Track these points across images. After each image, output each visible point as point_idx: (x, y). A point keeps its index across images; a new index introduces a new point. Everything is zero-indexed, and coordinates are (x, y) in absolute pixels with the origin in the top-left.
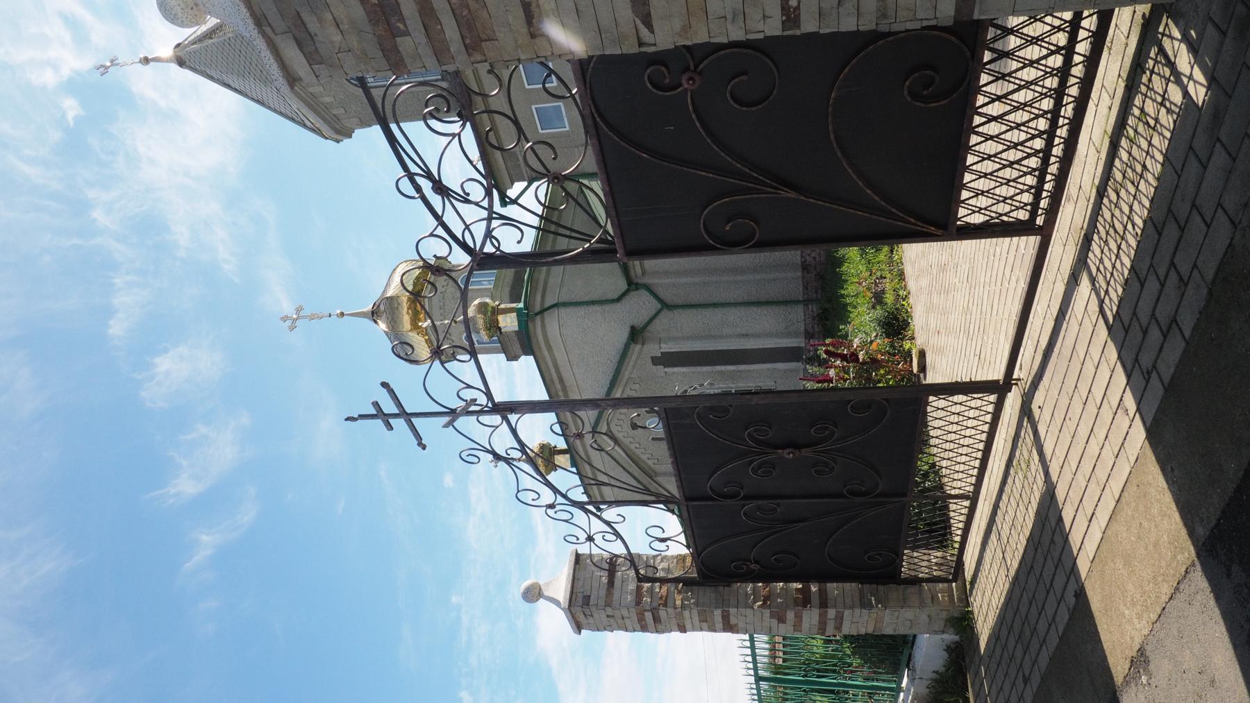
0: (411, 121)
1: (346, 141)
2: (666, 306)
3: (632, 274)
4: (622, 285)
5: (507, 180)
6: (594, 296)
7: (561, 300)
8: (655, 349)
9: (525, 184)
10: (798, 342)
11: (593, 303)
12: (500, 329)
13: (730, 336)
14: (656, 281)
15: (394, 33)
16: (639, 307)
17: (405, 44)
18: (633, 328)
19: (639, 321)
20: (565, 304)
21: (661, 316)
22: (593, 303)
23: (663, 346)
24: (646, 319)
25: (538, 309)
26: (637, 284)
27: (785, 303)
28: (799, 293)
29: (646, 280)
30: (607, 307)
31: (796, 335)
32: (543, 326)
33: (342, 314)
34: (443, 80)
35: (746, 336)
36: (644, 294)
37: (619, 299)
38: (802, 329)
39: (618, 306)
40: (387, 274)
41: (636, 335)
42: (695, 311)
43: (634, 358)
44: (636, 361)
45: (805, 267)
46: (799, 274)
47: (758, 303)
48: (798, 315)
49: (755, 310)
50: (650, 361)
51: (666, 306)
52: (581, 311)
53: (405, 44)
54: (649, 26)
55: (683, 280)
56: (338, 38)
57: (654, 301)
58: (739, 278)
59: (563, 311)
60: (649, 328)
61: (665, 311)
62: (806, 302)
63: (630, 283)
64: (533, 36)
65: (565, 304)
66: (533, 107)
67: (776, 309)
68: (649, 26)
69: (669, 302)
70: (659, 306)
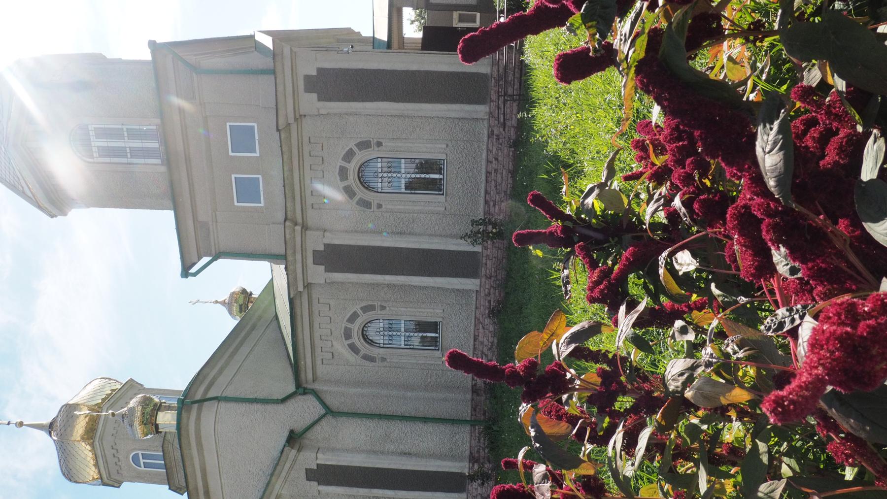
1: (60, 219)
2: (330, 411)
3: (303, 376)
4: (292, 388)
6: (260, 395)
7: (224, 395)
8: (310, 459)
9: (208, 259)
10: (462, 467)
11: (256, 401)
12: (157, 426)
13: (392, 453)
14: (325, 388)
16: (304, 410)
18: (292, 432)
19: (299, 426)
20: (227, 399)
21: (324, 422)
22: (256, 401)
23: (320, 455)
24: (308, 422)
25: (198, 397)
26: (305, 389)
27: (453, 421)
28: (466, 412)
29: (316, 386)
30: (269, 407)
31: (460, 459)
32: (198, 418)
33: (21, 424)
34: (162, 165)
35: (408, 454)
36: (310, 400)
37: (284, 400)
38: (467, 453)
39: (281, 407)
40: (74, 378)
41: (294, 439)
42: (359, 421)
43: (288, 465)
44: (289, 472)
45: (475, 390)
46: (469, 396)
47: (425, 420)
48: (464, 439)
49: (420, 426)
50: (303, 474)
51: (330, 411)
52: (243, 407)
55: (353, 390)
57: (317, 404)
58: (409, 394)
59: (223, 405)
60: (309, 435)
61: (329, 418)
62: (473, 423)
63: (298, 385)
65: (227, 399)
66: (233, 176)
67: (442, 427)
69: (334, 402)
70: (323, 412)
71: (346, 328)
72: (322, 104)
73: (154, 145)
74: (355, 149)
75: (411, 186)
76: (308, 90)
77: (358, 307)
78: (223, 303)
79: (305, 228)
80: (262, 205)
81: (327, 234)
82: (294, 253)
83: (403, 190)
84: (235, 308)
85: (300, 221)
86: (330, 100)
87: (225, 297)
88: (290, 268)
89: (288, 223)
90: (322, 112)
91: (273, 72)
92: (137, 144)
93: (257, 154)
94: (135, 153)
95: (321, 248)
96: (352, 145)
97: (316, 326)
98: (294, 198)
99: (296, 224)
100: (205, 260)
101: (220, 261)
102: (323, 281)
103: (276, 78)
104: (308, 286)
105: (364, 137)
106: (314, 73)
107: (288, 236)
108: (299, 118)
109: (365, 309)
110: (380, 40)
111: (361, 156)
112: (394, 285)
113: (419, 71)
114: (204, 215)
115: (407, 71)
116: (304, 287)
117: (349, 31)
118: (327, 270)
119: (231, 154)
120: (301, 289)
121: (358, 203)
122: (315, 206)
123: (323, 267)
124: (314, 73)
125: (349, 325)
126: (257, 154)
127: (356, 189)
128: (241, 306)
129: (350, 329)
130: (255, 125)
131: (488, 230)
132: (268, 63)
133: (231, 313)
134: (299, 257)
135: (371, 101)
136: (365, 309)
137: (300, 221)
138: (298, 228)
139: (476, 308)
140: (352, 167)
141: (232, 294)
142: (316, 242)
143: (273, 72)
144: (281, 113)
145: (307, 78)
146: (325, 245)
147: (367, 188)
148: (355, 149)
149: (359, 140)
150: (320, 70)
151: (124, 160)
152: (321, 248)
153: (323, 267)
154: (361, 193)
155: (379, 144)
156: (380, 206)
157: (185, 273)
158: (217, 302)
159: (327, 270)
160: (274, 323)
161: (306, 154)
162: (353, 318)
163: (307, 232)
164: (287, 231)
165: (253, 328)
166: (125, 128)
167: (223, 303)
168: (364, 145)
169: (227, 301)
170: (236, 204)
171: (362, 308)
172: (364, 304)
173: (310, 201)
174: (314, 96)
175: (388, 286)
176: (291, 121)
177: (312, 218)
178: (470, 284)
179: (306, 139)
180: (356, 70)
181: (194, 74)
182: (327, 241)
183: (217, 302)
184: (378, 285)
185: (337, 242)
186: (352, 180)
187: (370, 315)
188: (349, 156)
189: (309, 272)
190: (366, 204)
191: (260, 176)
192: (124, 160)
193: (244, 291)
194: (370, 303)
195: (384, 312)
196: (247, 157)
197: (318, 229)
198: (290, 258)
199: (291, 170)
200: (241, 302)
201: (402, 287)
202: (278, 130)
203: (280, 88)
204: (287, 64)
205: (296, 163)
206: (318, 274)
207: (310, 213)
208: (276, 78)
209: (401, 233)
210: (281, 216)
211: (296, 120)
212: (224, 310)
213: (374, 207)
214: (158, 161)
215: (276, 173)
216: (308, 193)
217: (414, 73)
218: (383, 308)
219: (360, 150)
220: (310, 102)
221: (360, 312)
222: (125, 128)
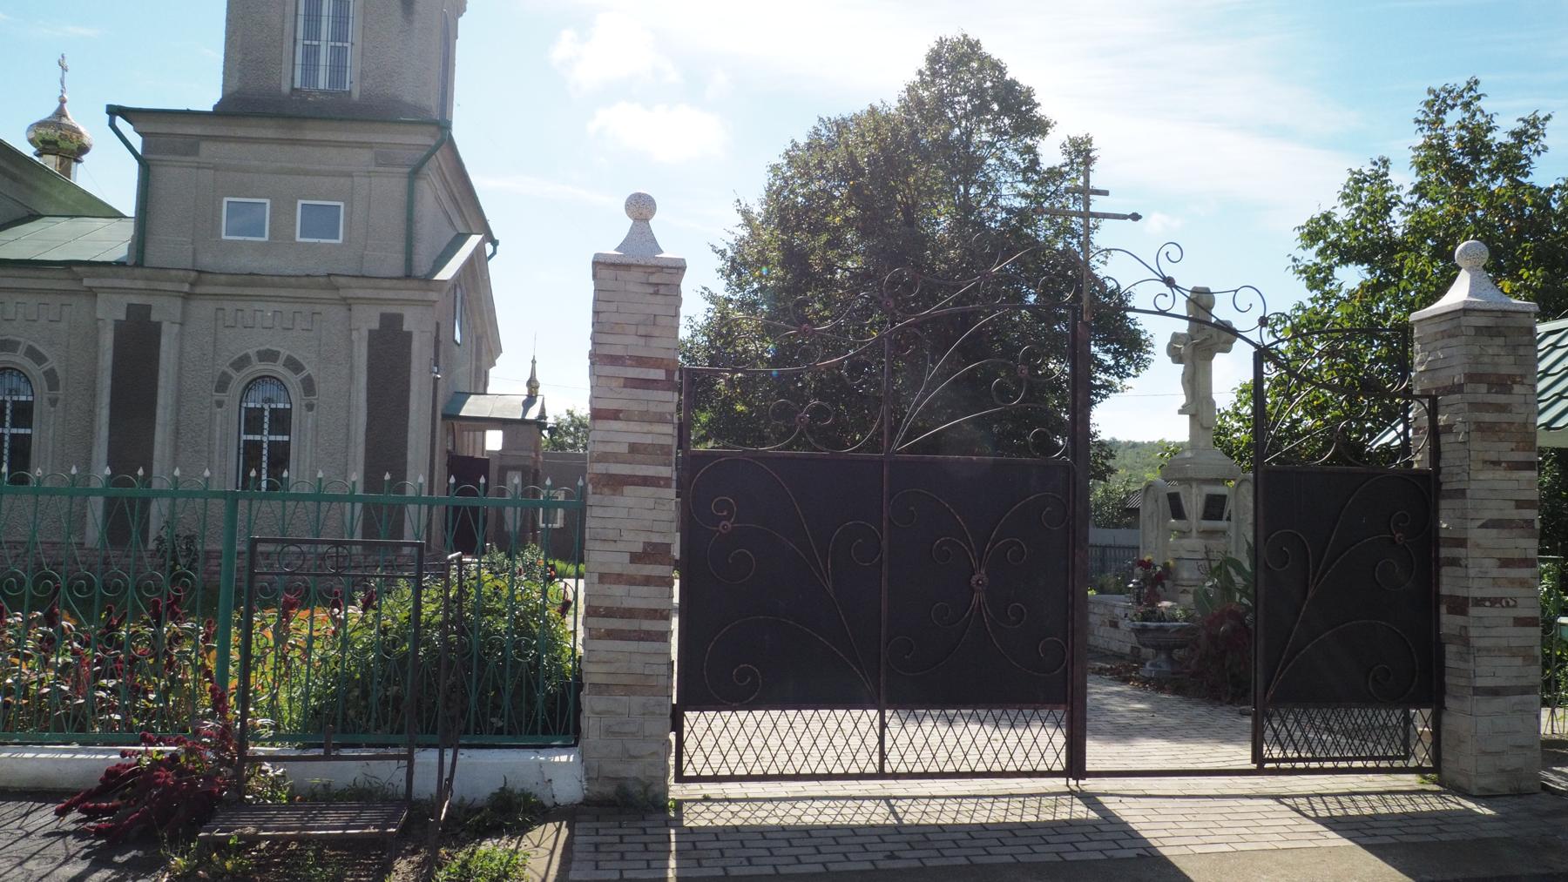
0: (229, 20)
5: (150, 128)
15: (1491, 385)
17: (1483, 388)
34: (293, 89)
53: (1483, 388)
54: (1483, 526)
56: (1490, 351)
64: (1485, 462)
68: (1483, 526)
71: (19, 343)
72: (365, 334)
73: (323, 82)
74: (304, 374)
75: (251, 453)
76: (384, 318)
77: (55, 365)
78: (60, 113)
79: (187, 297)
80: (224, 237)
81: (176, 328)
82: (147, 279)
83: (244, 437)
84: (51, 134)
85: (198, 290)
86: (370, 346)
87: (74, 118)
88: (122, 271)
89: (193, 275)
90: (355, 335)
91: (408, 276)
92: (324, 58)
93: (298, 239)
94: (311, 54)
95: (155, 317)
96: (309, 370)
97: (21, 298)
98: (233, 285)
99: (192, 285)
100: (137, 141)
101: (135, 164)
102: (99, 315)
103: (398, 278)
104: (92, 293)
105: (320, 387)
106: (405, 328)
107: (173, 273)
108: (347, 303)
109: (51, 376)
110: (464, 403)
111: (293, 381)
112: (92, 420)
113: (405, 463)
114: (206, 149)
115: (406, 448)
116: (90, 288)
117: (496, 350)
118: (118, 323)
119: (300, 202)
120: (86, 282)
121: (224, 373)
122: (220, 314)
123: (123, 317)
124: (405, 328)
125: (22, 349)
126: (298, 239)
127: (246, 371)
128: (55, 143)
129: (14, 350)
130: (340, 241)
131: (181, 553)
132: (421, 268)
133: (41, 124)
134: (140, 284)
135: (368, 400)
136: (51, 376)
137: (198, 290)
138: (186, 288)
139: (54, 544)
140: (279, 369)
141: (75, 130)
142: (165, 311)
143: (408, 276)
144: (353, 282)
145: (399, 318)
146: (158, 325)
147: (247, 388)
148: (304, 374)
149: (316, 379)
150: (409, 335)
151: (300, 35)
152: (155, 317)
153: (123, 317)
154: (239, 379)
155: (310, 407)
156: (220, 404)
157: (114, 111)
158: (63, 101)
159: (118, 323)
160: (23, 213)
161: (296, 307)
162: (38, 358)
163: (179, 302)
164: (181, 273)
165: (14, 178)
166: (348, 45)
167: (60, 113)
168: (309, 386)
169: (64, 121)
170: (226, 200)
171: (52, 370)
172: (60, 374)
173: (229, 306)
174: (376, 325)
175: (91, 413)
176: (343, 293)
177: (202, 310)
178: (94, 532)
179: (318, 308)
180: (408, 382)
181: (408, 170)
182: (165, 327)
183: (63, 101)
184: (94, 396)
185: (164, 341)
186: (259, 368)
187: (40, 383)
188: (294, 365)
189: (115, 297)
190: (223, 384)
191: (266, 238)
192: (300, 35)
193: (84, 149)
194: (61, 384)
195: (45, 402)
196: (294, 225)
197: (184, 313)
198: (138, 271)
199: (274, 286)
200: (63, 144)
201: (90, 431)
202: (329, 275)
203: (386, 283)
204: (417, 295)
205: (283, 292)
206: (111, 310)
207: (211, 306)
208: (398, 278)
209: (177, 432)
210: (207, 261)
211: (345, 299)
212: (46, 111)
213: (218, 396)
214: (297, 85)
215: (270, 264)
216: (240, 305)
217: (404, 455)
218: (53, 402)
219: (303, 381)
220: (368, 319)
221: (46, 367)
222: (348, 45)
